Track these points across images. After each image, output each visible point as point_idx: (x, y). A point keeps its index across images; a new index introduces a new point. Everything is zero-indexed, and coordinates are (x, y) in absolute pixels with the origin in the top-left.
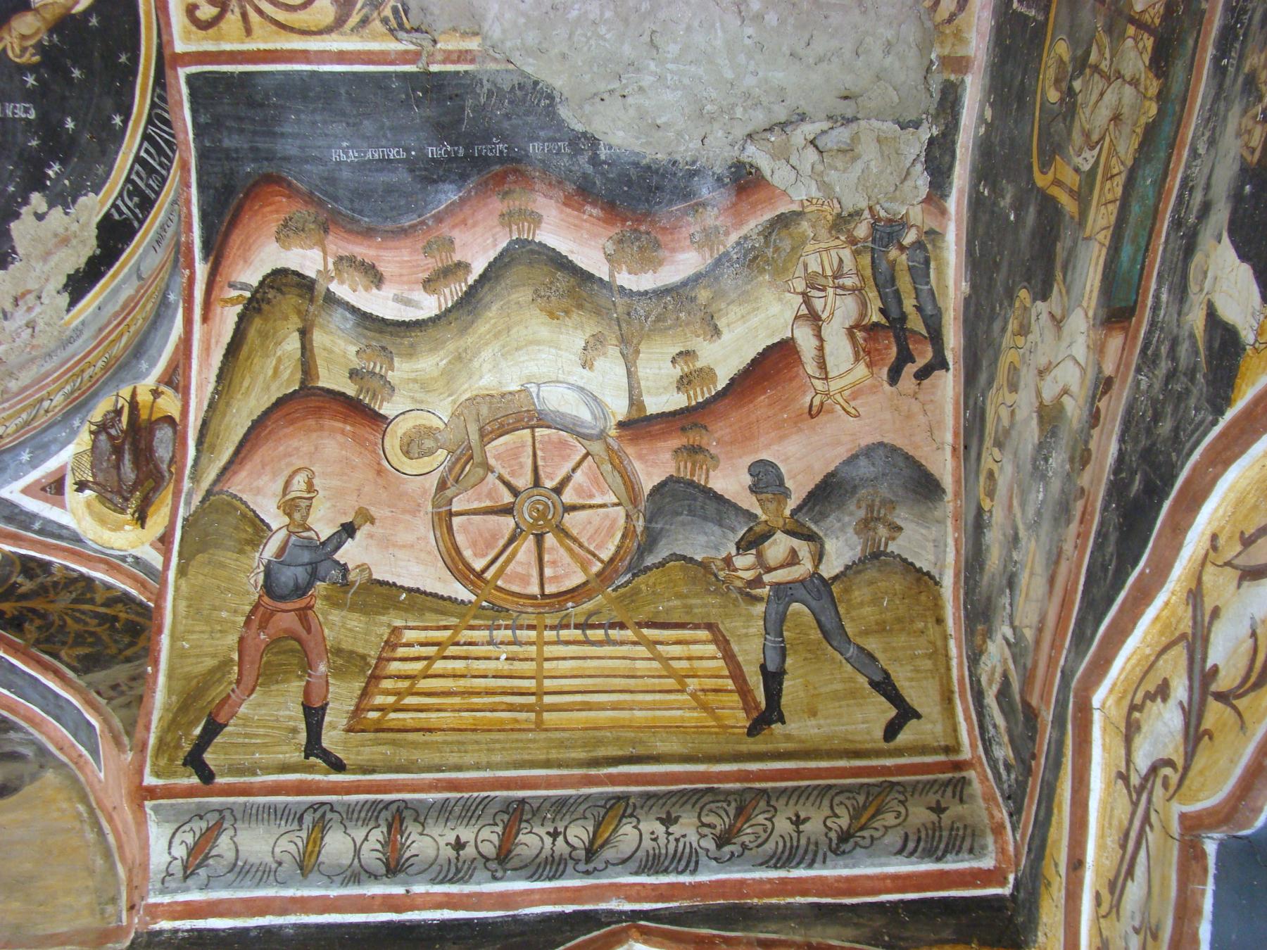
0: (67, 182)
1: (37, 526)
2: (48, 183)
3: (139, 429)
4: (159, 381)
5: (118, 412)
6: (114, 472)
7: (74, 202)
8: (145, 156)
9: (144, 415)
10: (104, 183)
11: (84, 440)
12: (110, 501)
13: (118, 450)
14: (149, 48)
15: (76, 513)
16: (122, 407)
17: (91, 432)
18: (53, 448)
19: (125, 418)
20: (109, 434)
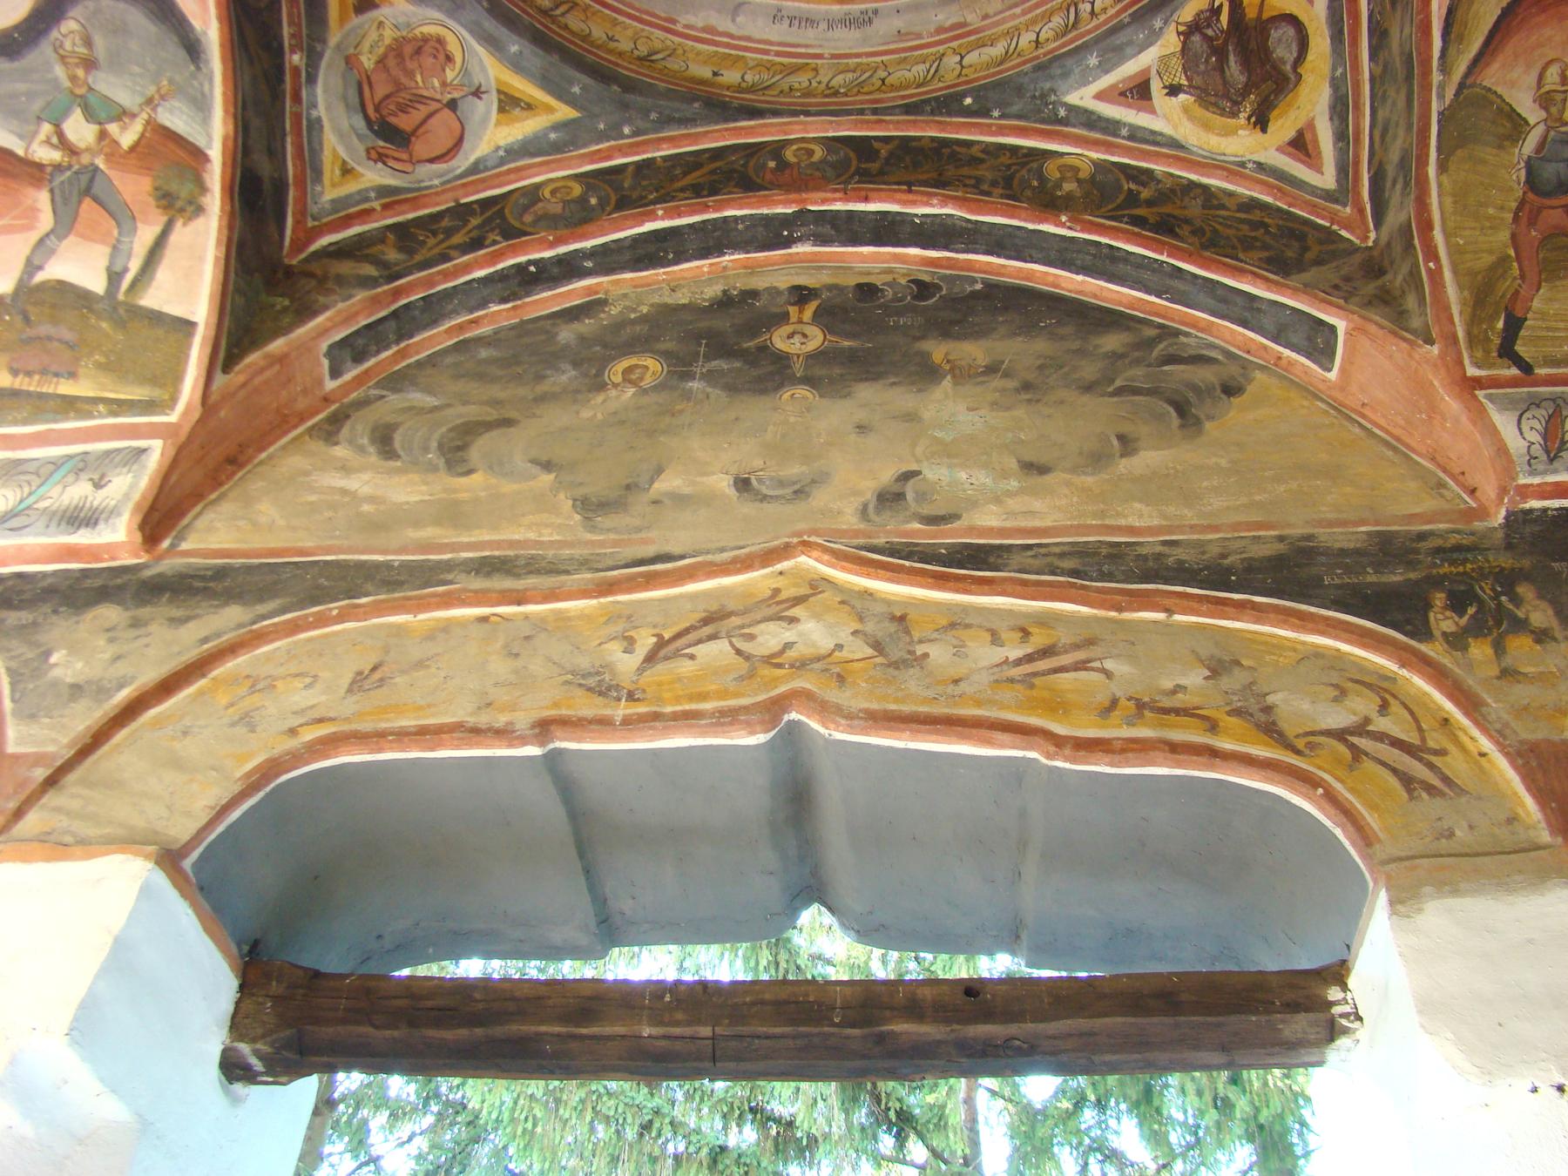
1: (1124, 132)
5: (1215, 12)
6: (1217, 75)
9: (1251, 14)
11: (1170, 42)
12: (1215, 104)
15: (1170, 117)
16: (1221, 5)
17: (1179, 34)
18: (1129, 51)
19: (1224, 18)
20: (1205, 37)
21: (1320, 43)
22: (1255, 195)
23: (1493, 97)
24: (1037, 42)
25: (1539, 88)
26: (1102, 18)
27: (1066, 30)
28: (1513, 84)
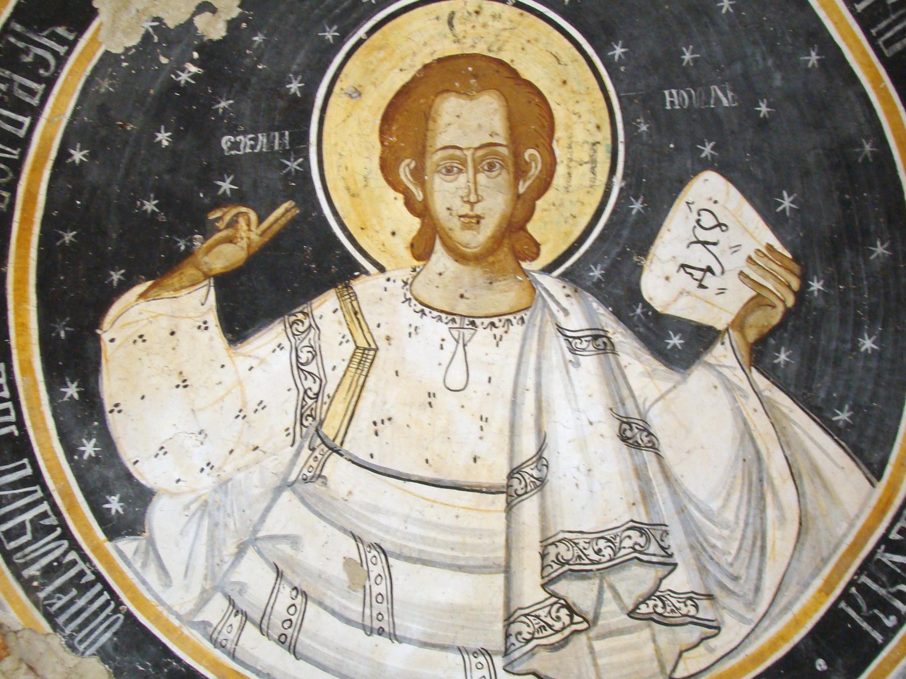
0: (164, 60)
2: (196, 55)
7: (147, 37)
8: (20, 118)
10: (96, 69)
14: (23, 257)
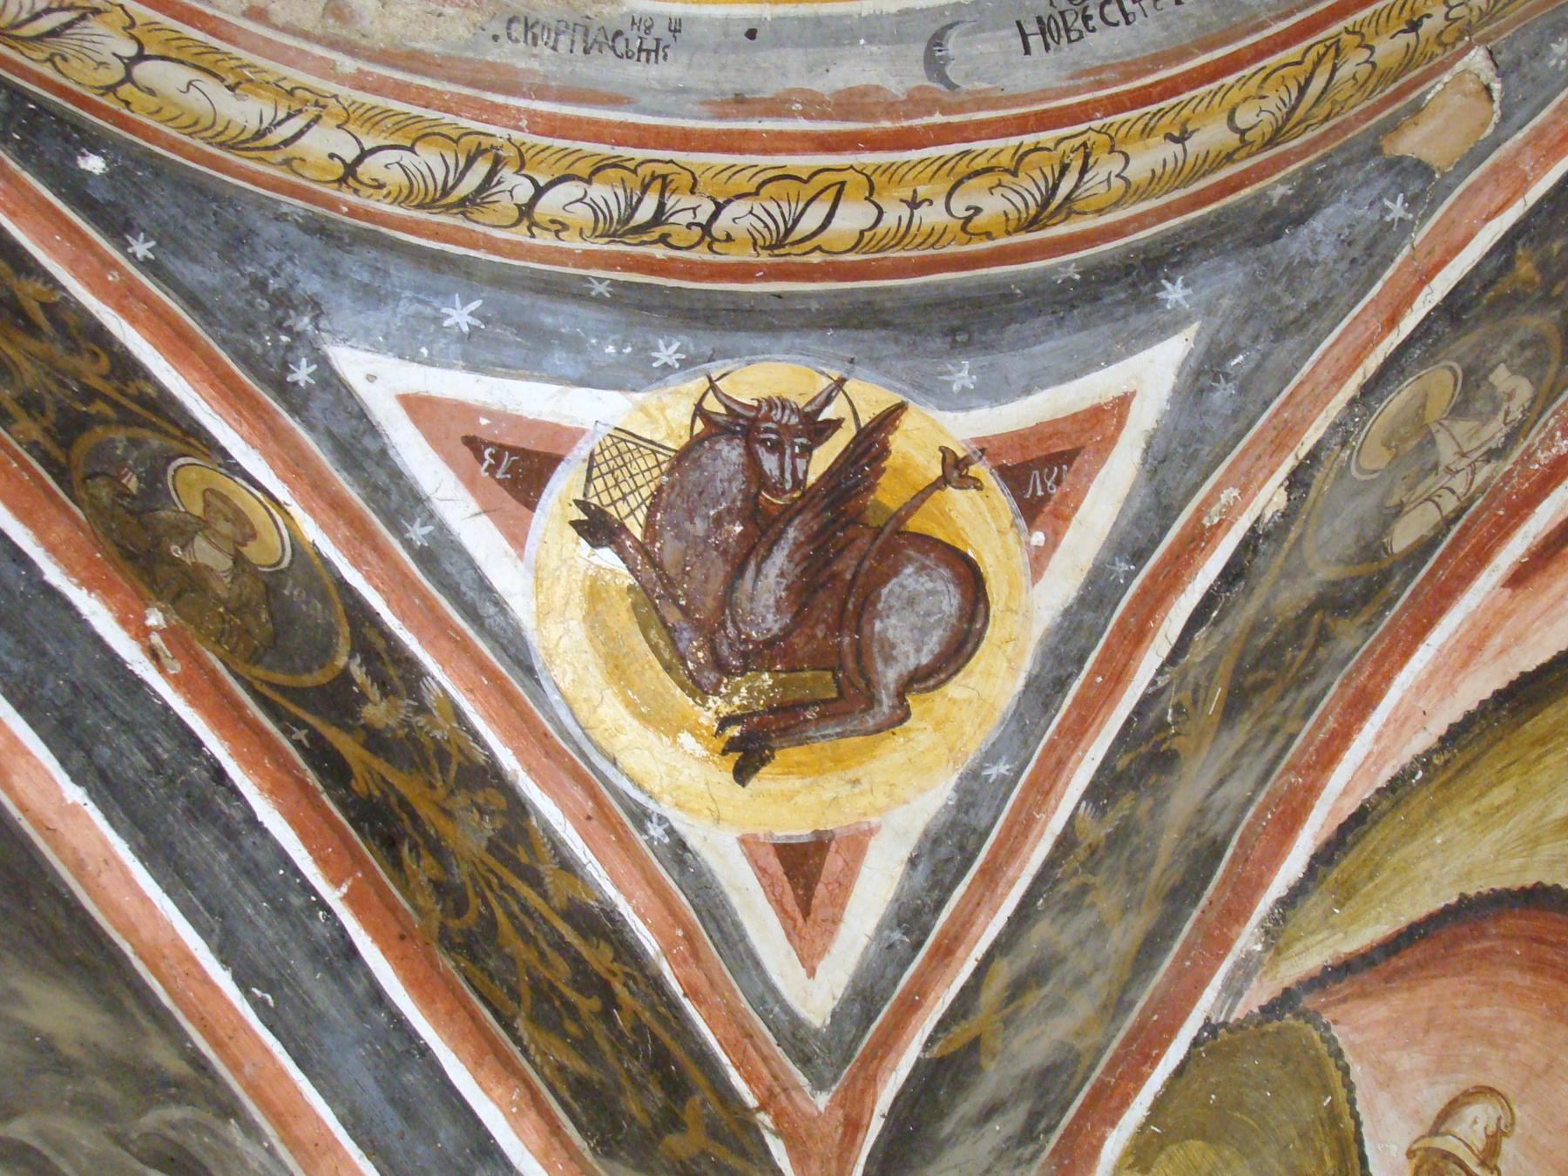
1: (419, 532)
3: (857, 518)
4: (984, 448)
5: (816, 430)
9: (889, 494)
11: (667, 413)
12: (671, 633)
13: (762, 524)
15: (550, 583)
16: (836, 424)
17: (699, 412)
18: (559, 359)
19: (824, 457)
20: (753, 463)
21: (996, 677)
22: (625, 909)
23: (1337, 1076)
24: (351, 169)
25: (1435, 1131)
26: (544, 239)
27: (438, 199)
28: (1389, 1080)
